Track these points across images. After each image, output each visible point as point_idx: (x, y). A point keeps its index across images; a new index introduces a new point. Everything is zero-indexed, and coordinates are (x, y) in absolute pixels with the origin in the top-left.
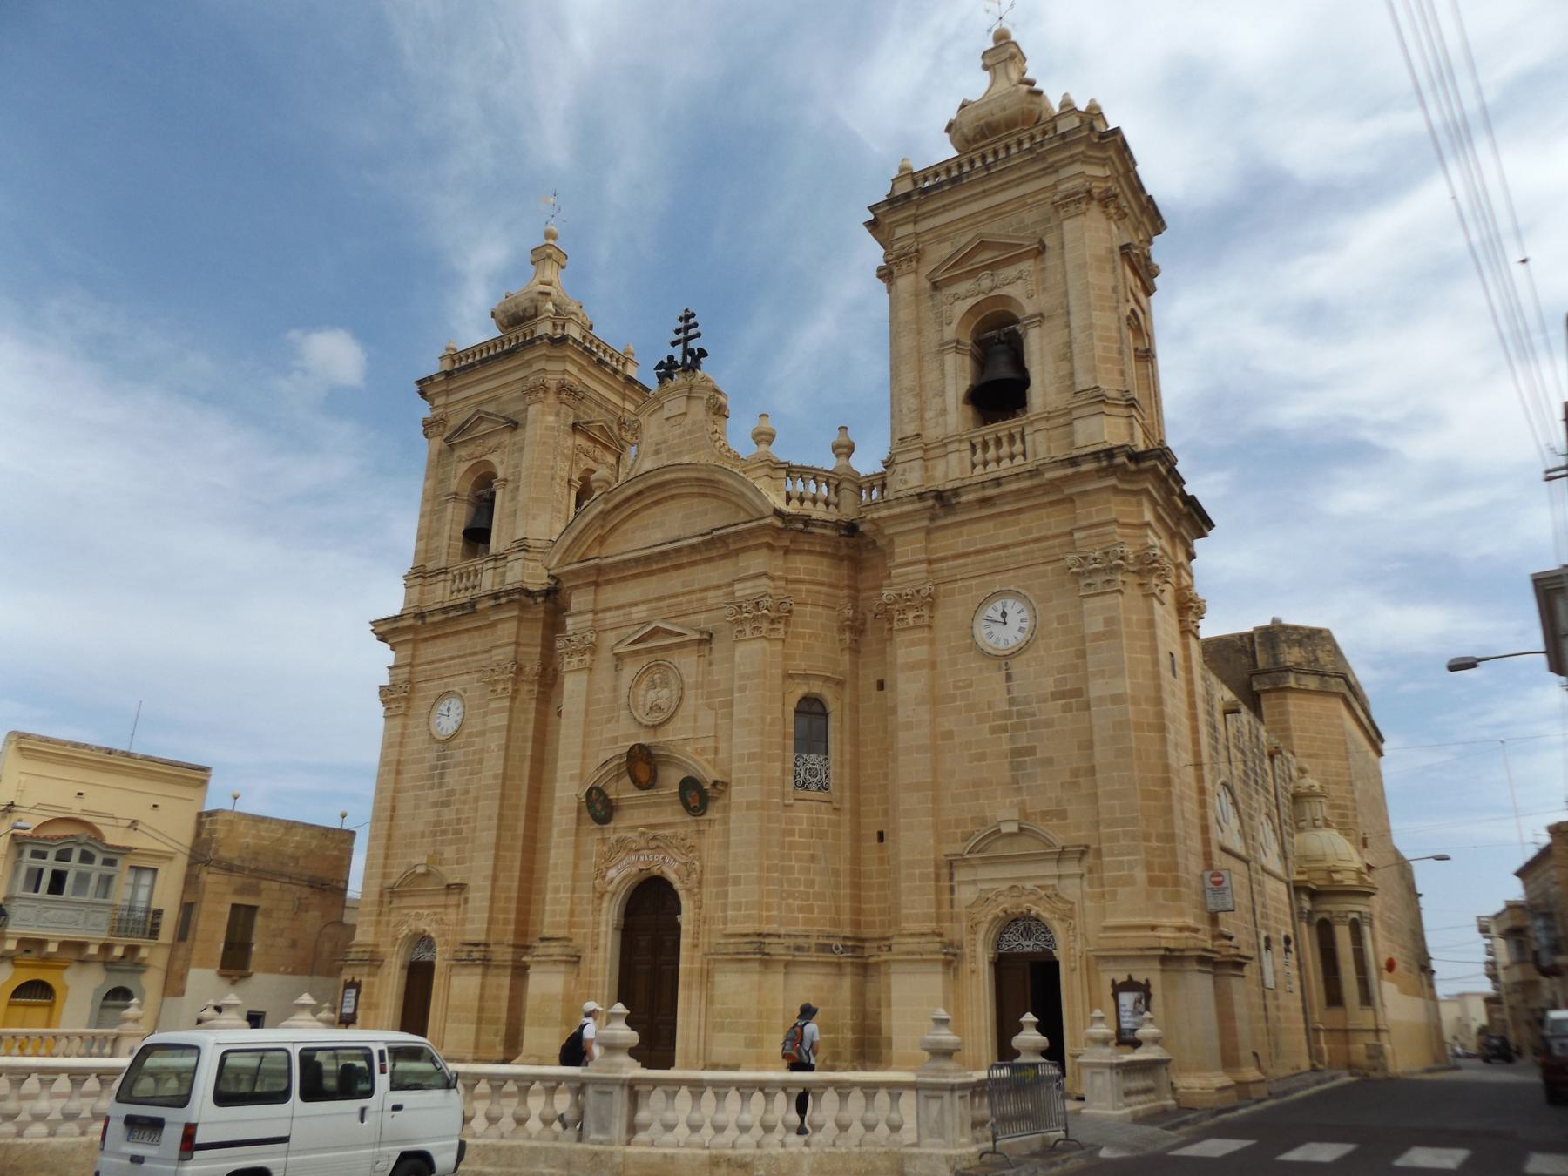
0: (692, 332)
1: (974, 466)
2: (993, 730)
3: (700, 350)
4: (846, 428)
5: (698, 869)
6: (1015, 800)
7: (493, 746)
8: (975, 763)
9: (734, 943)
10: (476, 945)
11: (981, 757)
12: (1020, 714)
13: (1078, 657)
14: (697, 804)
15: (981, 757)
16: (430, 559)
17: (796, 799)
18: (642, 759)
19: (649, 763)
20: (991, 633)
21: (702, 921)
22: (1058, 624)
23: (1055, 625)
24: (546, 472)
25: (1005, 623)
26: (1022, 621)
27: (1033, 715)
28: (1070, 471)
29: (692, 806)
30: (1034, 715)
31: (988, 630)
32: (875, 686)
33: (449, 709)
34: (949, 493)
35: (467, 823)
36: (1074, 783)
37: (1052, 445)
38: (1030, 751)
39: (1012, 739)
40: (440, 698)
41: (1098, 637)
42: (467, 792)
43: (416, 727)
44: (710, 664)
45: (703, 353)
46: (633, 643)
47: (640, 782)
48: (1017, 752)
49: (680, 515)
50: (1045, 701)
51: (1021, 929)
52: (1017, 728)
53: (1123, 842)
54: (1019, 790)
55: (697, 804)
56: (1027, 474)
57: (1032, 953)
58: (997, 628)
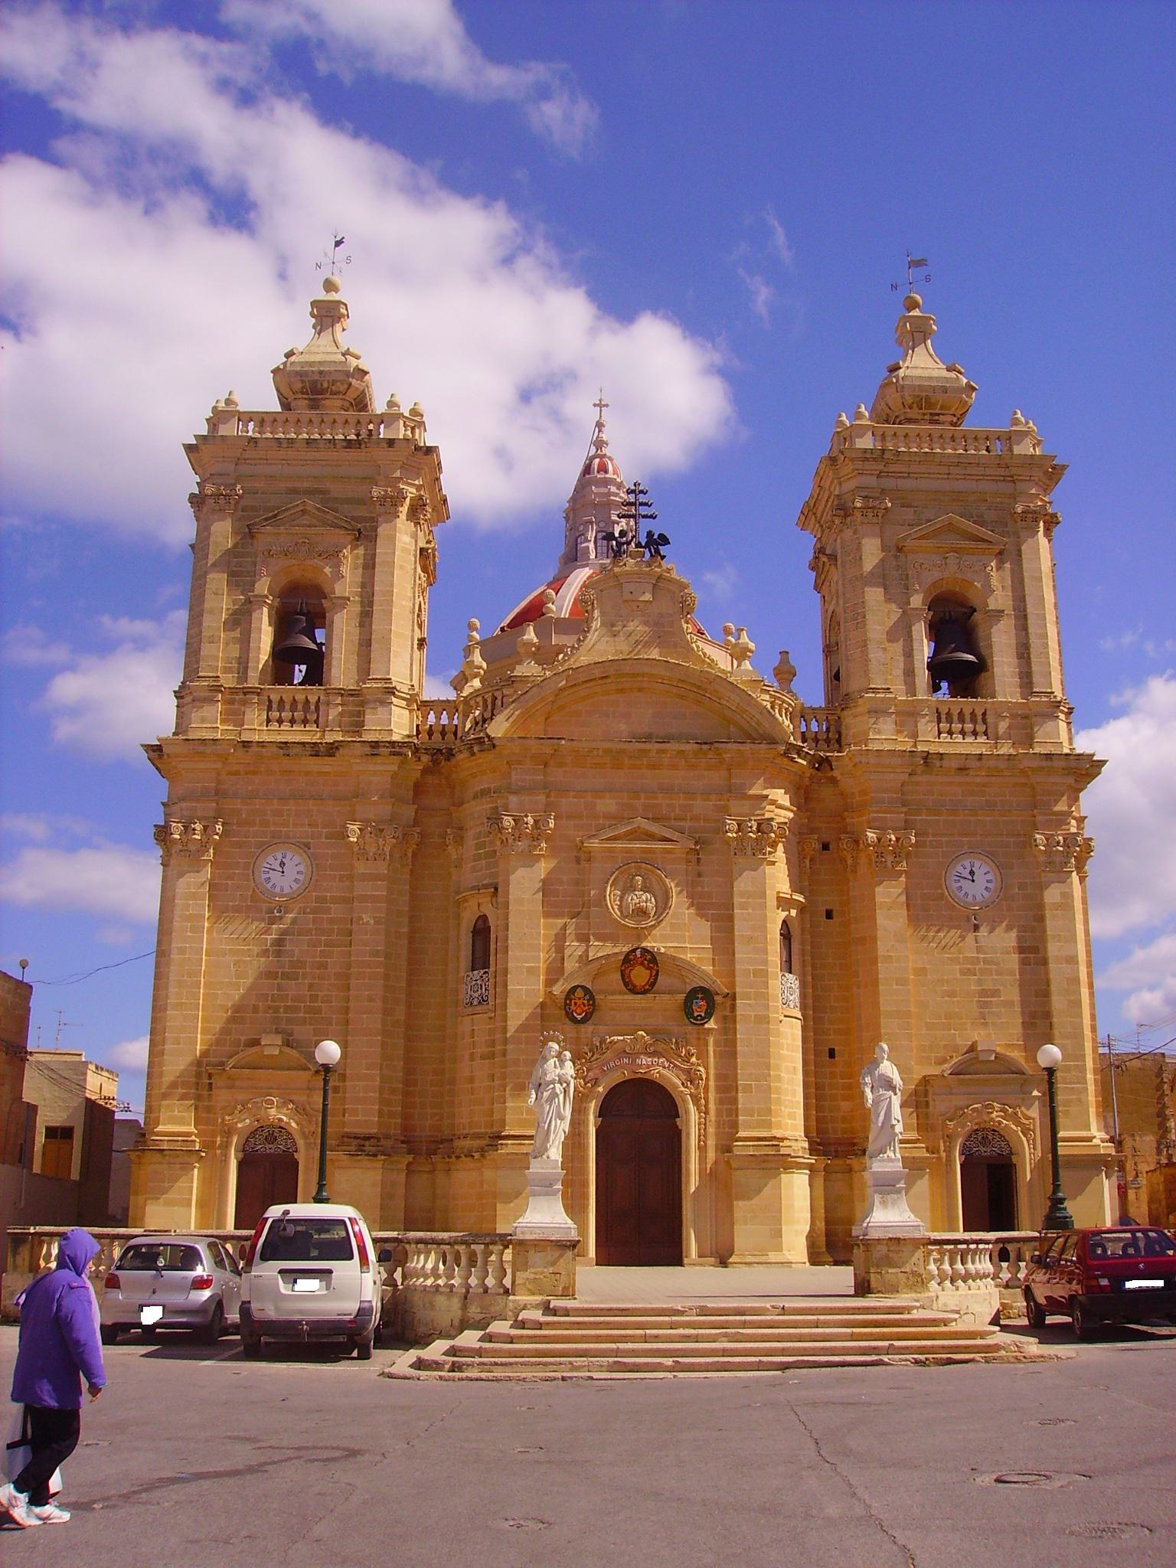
0: (644, 511)
1: (940, 733)
2: (963, 972)
3: (661, 536)
4: (787, 653)
5: (704, 1077)
6: (982, 1033)
7: (366, 918)
8: (946, 998)
9: (753, 1146)
10: (368, 1138)
11: (951, 994)
12: (985, 961)
13: (1035, 921)
14: (703, 1015)
15: (951, 994)
16: (226, 670)
17: (785, 1016)
18: (642, 964)
19: (649, 968)
20: (961, 887)
21: (703, 1126)
22: (1019, 889)
23: (1017, 890)
24: (404, 603)
25: (973, 881)
26: (988, 881)
27: (997, 964)
28: (1044, 764)
29: (696, 1014)
30: (997, 964)
31: (959, 884)
32: (834, 913)
33: (282, 864)
34: (935, 756)
35: (328, 1001)
36: (1032, 1023)
37: (1012, 732)
38: (995, 993)
39: (979, 982)
40: (264, 847)
41: (1058, 906)
42: (324, 966)
43: (229, 878)
44: (699, 875)
45: (664, 540)
46: (607, 839)
47: (635, 986)
48: (983, 993)
49: (651, 711)
50: (1008, 953)
51: (980, 1138)
52: (983, 972)
53: (1074, 1073)
54: (985, 1024)
55: (703, 1015)
56: (1006, 757)
57: (990, 1157)
58: (963, 883)
